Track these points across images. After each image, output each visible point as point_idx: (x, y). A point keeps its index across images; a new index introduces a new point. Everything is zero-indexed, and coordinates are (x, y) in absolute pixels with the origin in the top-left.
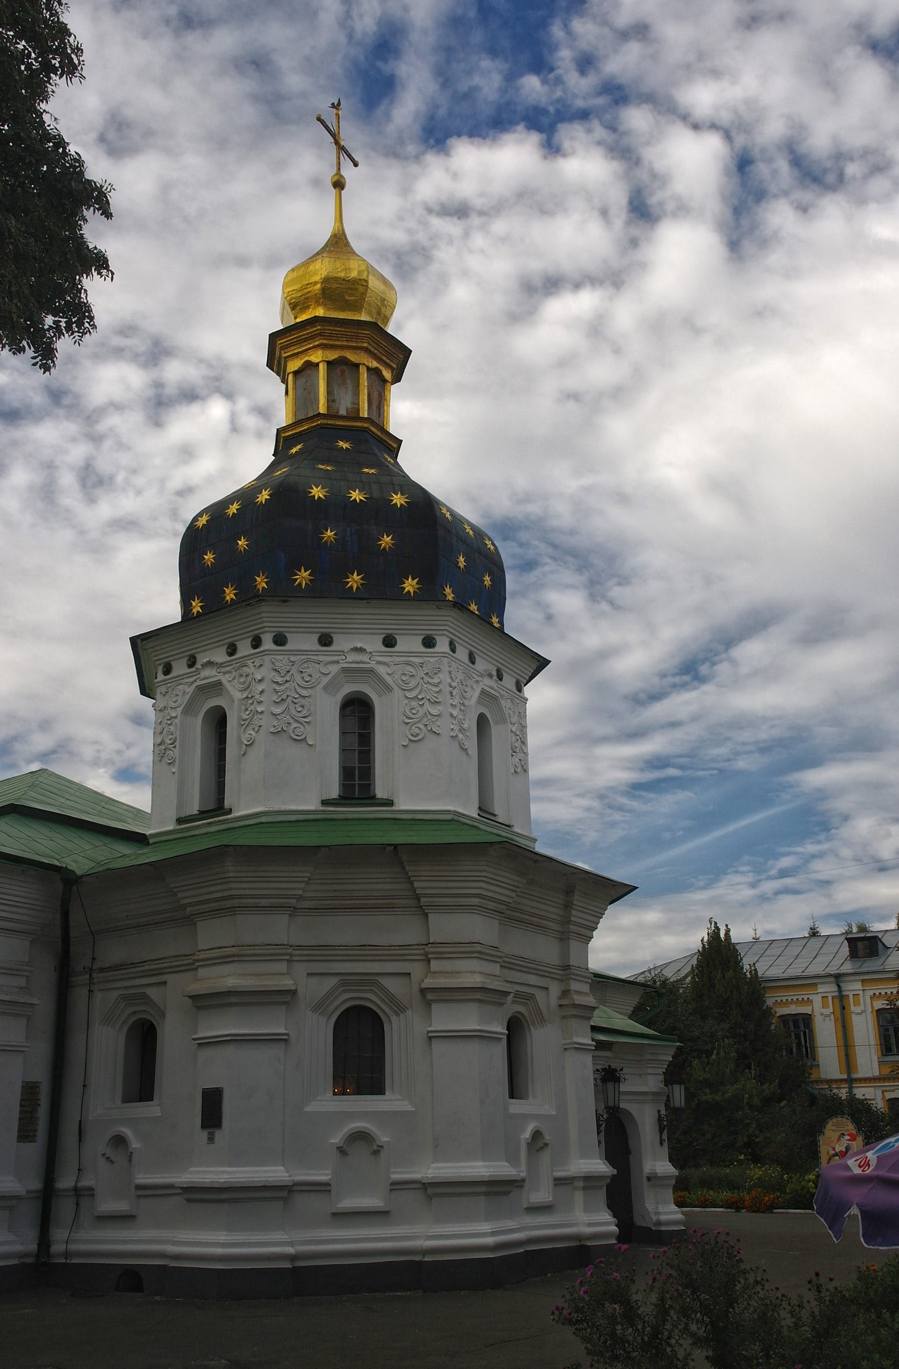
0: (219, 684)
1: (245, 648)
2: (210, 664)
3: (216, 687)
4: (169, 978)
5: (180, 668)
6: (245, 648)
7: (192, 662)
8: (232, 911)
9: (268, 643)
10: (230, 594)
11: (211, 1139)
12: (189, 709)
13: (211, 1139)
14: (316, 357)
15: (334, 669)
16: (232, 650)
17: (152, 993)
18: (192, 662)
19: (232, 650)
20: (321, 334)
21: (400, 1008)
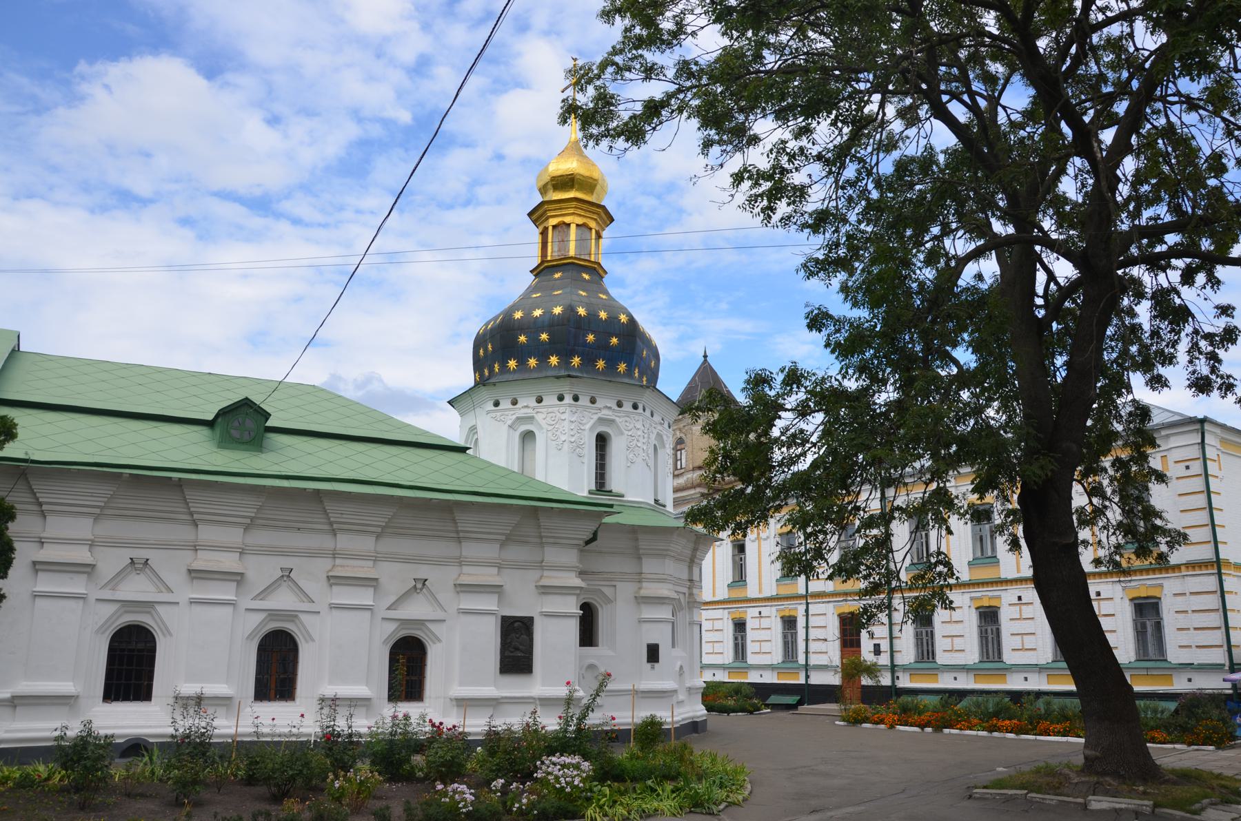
0: (613, 421)
1: (627, 406)
2: (610, 408)
3: (611, 422)
4: (619, 584)
5: (585, 400)
6: (627, 406)
7: (593, 401)
8: (664, 556)
9: (640, 410)
10: (601, 364)
11: (653, 668)
12: (591, 429)
13: (653, 668)
14: (592, 224)
15: (655, 432)
16: (620, 405)
17: (605, 590)
18: (593, 401)
19: (620, 405)
20: (598, 214)
21: (682, 609)
